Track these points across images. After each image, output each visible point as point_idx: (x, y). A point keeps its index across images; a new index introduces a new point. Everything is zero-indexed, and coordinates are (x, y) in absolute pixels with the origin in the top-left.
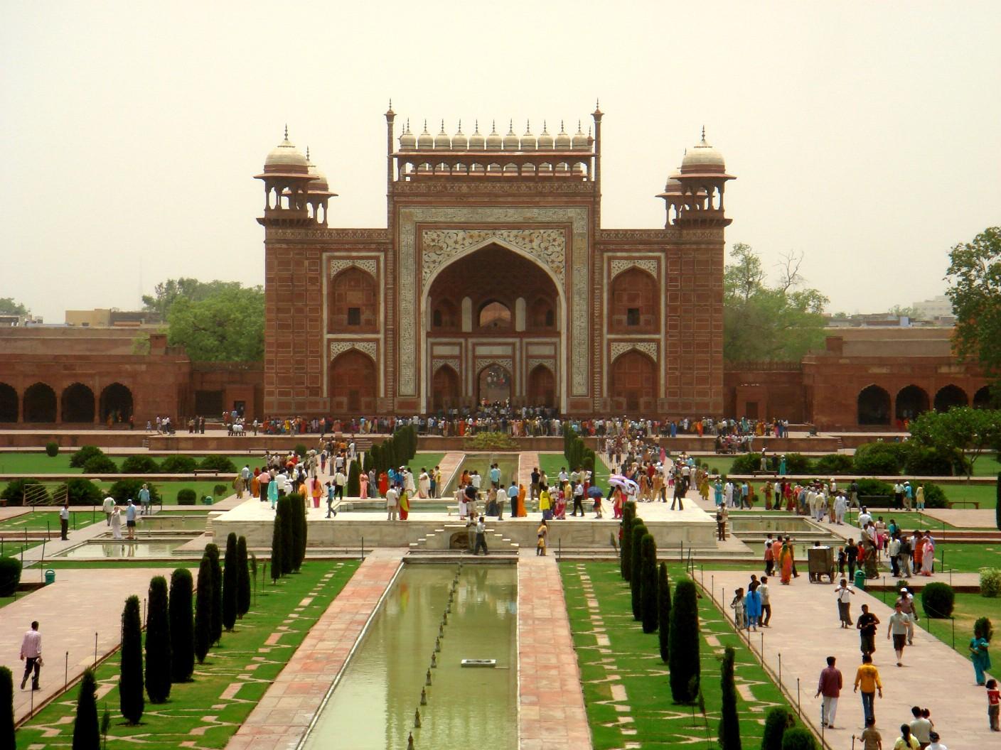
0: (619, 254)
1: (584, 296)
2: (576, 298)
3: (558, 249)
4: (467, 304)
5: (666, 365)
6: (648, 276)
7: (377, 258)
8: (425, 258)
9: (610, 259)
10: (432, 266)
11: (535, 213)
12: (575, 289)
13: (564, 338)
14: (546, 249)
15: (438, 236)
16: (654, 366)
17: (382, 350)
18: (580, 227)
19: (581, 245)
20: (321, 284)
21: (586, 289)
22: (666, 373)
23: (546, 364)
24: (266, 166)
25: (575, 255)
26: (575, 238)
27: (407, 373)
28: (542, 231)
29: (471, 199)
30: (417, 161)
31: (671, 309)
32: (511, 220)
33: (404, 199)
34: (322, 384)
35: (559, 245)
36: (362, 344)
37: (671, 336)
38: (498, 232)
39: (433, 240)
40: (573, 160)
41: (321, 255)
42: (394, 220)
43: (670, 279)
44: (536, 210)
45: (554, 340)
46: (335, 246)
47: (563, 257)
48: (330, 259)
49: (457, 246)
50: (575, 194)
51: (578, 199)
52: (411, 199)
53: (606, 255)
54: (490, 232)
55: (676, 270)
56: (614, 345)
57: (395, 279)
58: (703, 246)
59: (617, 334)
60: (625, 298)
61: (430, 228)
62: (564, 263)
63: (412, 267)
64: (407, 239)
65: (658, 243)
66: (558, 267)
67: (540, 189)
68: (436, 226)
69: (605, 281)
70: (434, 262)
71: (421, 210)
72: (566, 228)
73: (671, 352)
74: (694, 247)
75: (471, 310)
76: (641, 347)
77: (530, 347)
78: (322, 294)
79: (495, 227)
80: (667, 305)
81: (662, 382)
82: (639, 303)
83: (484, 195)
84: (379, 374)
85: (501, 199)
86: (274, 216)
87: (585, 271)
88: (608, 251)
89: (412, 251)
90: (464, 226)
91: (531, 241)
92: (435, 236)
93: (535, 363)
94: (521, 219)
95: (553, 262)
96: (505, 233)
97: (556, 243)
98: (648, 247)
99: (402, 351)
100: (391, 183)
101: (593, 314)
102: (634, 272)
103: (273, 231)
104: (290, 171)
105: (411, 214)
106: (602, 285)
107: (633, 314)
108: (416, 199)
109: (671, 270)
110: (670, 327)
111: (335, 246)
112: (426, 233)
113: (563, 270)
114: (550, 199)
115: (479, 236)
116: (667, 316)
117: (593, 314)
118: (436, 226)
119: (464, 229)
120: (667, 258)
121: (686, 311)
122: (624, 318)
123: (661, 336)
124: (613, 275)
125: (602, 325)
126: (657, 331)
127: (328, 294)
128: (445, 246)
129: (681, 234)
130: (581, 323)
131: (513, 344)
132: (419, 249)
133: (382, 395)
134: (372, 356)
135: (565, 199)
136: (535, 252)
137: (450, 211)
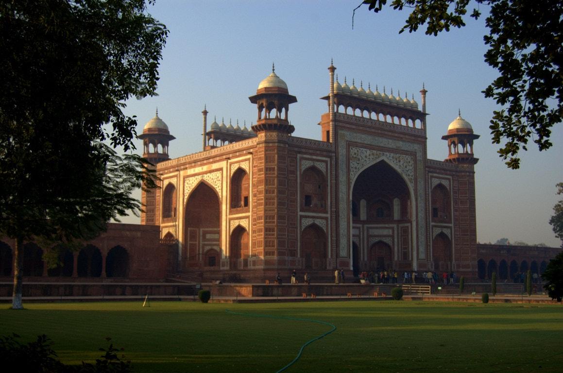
0: (435, 175)
2: (419, 199)
3: (411, 168)
7: (326, 162)
8: (351, 164)
10: (355, 170)
11: (400, 144)
12: (419, 193)
13: (414, 224)
14: (406, 167)
15: (358, 151)
16: (450, 242)
17: (329, 225)
18: (419, 155)
19: (420, 166)
20: (297, 176)
23: (385, 241)
27: (343, 241)
28: (404, 156)
32: (390, 146)
33: (341, 124)
34: (297, 248)
35: (411, 166)
36: (318, 220)
39: (355, 154)
41: (297, 156)
45: (391, 225)
46: (304, 150)
48: (302, 158)
51: (419, 139)
53: (430, 174)
54: (381, 152)
56: (434, 228)
57: (337, 177)
63: (345, 170)
64: (342, 151)
65: (450, 171)
66: (411, 179)
69: (430, 190)
77: (370, 230)
78: (297, 183)
80: (454, 207)
84: (328, 244)
85: (386, 133)
87: (422, 183)
90: (370, 147)
91: (400, 161)
92: (356, 151)
93: (377, 240)
94: (395, 147)
95: (409, 175)
97: (410, 164)
99: (340, 226)
111: (304, 150)
112: (352, 149)
123: (452, 225)
126: (451, 223)
127: (300, 183)
128: (361, 159)
130: (421, 215)
131: (359, 228)
133: (330, 257)
134: (323, 228)
135: (413, 138)
137: (363, 136)
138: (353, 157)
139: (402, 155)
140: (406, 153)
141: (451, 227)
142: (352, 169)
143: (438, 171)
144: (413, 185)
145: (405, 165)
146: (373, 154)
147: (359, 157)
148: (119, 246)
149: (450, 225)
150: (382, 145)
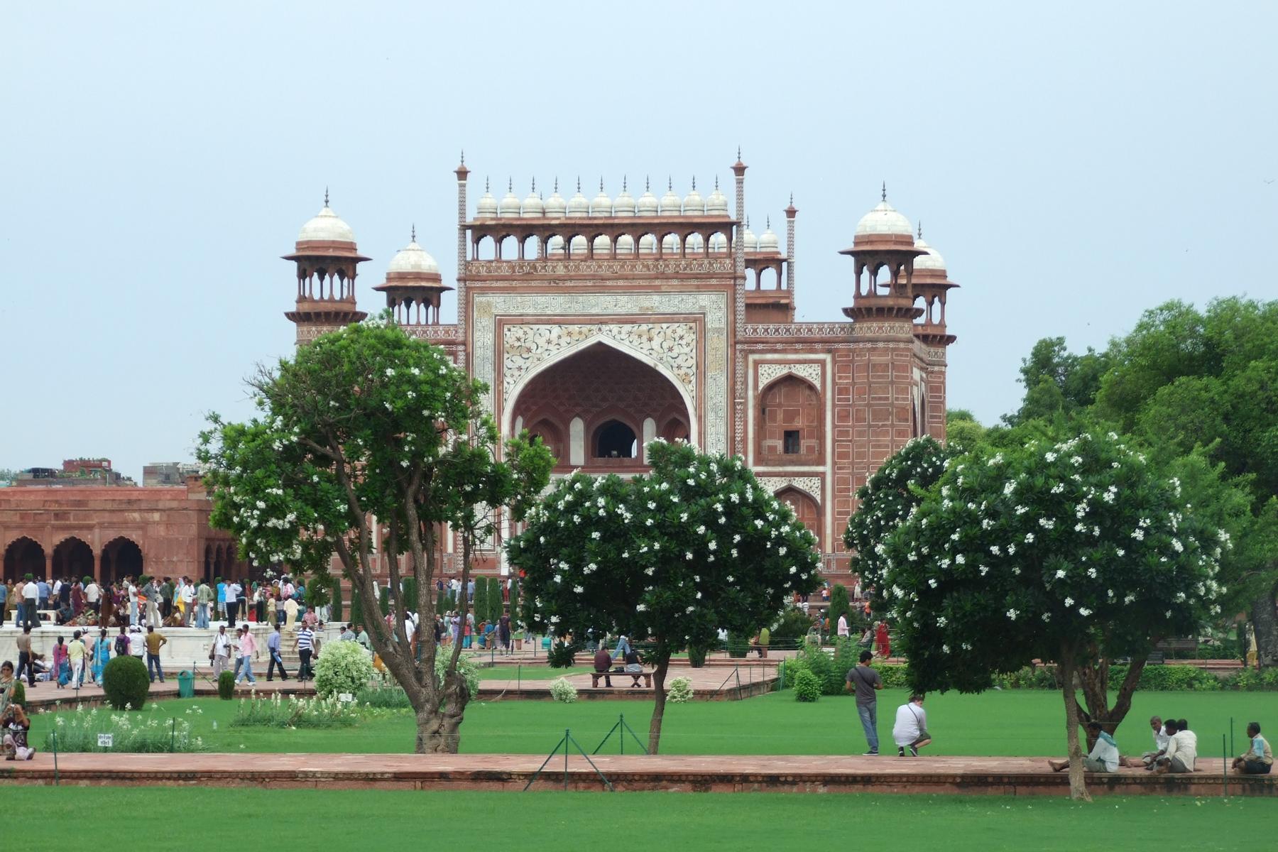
0: (769, 356)
1: (722, 413)
2: (711, 417)
3: (687, 350)
4: (577, 429)
5: (833, 508)
6: (811, 387)
8: (507, 363)
9: (757, 363)
10: (516, 373)
11: (655, 302)
12: (709, 404)
14: (671, 349)
15: (525, 333)
16: (819, 510)
19: (718, 345)
21: (724, 404)
22: (834, 519)
24: (298, 243)
25: (710, 358)
26: (709, 335)
28: (665, 326)
29: (568, 284)
30: (500, 230)
31: (840, 433)
32: (623, 311)
33: (479, 284)
35: (688, 345)
37: (839, 468)
38: (604, 327)
39: (519, 340)
40: (708, 228)
42: (466, 312)
43: (840, 391)
44: (656, 298)
47: (694, 361)
49: (551, 347)
50: (710, 276)
51: (714, 282)
52: (488, 284)
53: (751, 358)
54: (595, 327)
55: (847, 378)
58: (881, 345)
59: (767, 465)
60: (780, 416)
61: (514, 323)
62: (694, 368)
64: (483, 339)
66: (686, 374)
67: (661, 269)
68: (521, 320)
69: (750, 393)
70: (520, 368)
71: (502, 299)
72: (697, 320)
73: (840, 491)
74: (869, 345)
75: (582, 434)
76: (799, 483)
79: (601, 321)
80: (834, 426)
81: (829, 531)
82: (799, 423)
83: (584, 278)
86: (306, 307)
88: (753, 352)
89: (490, 353)
91: (650, 340)
92: (520, 333)
94: (636, 310)
95: (679, 367)
96: (615, 328)
97: (683, 342)
98: (806, 346)
100: (466, 265)
101: (733, 439)
102: (790, 381)
103: (305, 329)
104: (328, 248)
105: (489, 304)
106: (746, 398)
107: (791, 438)
108: (495, 284)
109: (840, 378)
110: (839, 455)
113: (693, 379)
114: (675, 282)
115: (580, 333)
116: (834, 441)
117: (733, 439)
118: (521, 320)
119: (559, 323)
120: (834, 362)
121: (861, 434)
122: (779, 444)
123: (827, 469)
124: (761, 387)
125: (746, 454)
126: (821, 461)
129: (853, 329)
132: (499, 351)
133: (450, 549)
135: (696, 282)
136: (655, 355)
138: (512, 347)
139: (657, 326)
140: (671, 318)
141: (824, 473)
142: (508, 373)
143: (779, 346)
144: (692, 387)
145: (665, 345)
146: (569, 334)
147: (527, 345)
148: (122, 538)
149: (820, 469)
150: (593, 311)
